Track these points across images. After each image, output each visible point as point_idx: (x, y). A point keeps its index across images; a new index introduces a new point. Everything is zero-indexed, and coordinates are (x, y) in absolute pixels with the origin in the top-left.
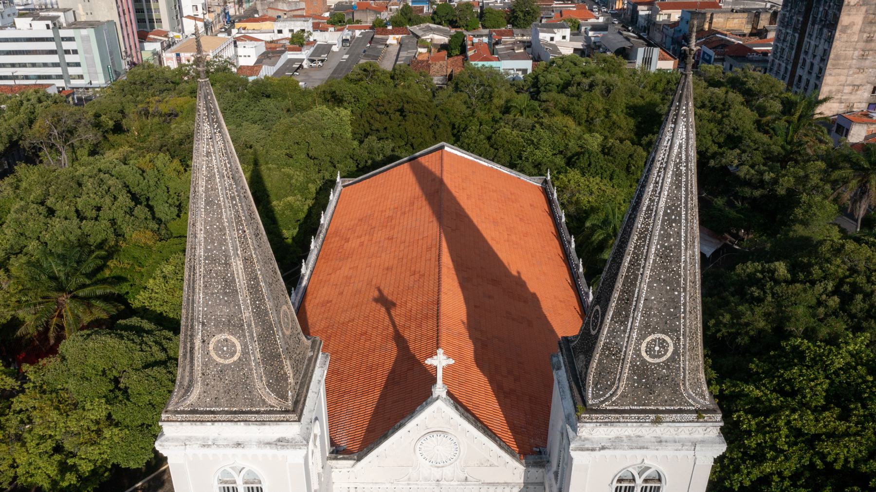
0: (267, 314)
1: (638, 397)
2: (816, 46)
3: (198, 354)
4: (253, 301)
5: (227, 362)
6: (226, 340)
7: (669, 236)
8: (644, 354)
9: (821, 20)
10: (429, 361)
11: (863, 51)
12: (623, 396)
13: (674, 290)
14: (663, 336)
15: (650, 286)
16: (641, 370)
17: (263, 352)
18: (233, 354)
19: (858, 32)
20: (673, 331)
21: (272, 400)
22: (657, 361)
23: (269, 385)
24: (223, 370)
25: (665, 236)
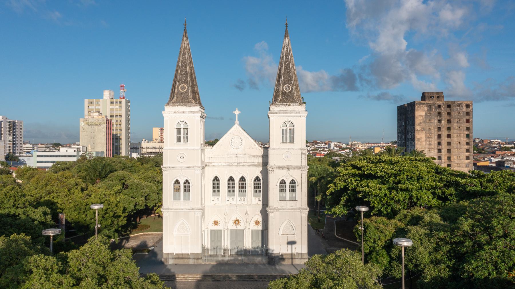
0: (194, 82)
1: (284, 101)
2: (411, 149)
3: (176, 89)
4: (191, 77)
5: (183, 91)
6: (184, 86)
7: (287, 62)
8: (284, 89)
9: (410, 139)
10: (234, 112)
11: (429, 149)
12: (280, 100)
13: (290, 74)
14: (288, 85)
15: (284, 73)
16: (284, 94)
17: (192, 90)
18: (185, 89)
19: (424, 141)
20: (291, 84)
21: (193, 101)
22: (288, 91)
23: (193, 99)
24: (182, 93)
25: (286, 62)
